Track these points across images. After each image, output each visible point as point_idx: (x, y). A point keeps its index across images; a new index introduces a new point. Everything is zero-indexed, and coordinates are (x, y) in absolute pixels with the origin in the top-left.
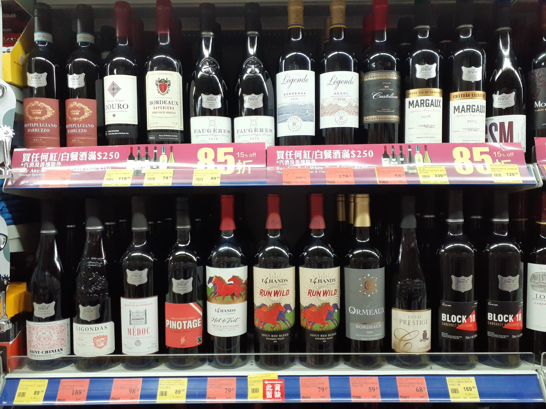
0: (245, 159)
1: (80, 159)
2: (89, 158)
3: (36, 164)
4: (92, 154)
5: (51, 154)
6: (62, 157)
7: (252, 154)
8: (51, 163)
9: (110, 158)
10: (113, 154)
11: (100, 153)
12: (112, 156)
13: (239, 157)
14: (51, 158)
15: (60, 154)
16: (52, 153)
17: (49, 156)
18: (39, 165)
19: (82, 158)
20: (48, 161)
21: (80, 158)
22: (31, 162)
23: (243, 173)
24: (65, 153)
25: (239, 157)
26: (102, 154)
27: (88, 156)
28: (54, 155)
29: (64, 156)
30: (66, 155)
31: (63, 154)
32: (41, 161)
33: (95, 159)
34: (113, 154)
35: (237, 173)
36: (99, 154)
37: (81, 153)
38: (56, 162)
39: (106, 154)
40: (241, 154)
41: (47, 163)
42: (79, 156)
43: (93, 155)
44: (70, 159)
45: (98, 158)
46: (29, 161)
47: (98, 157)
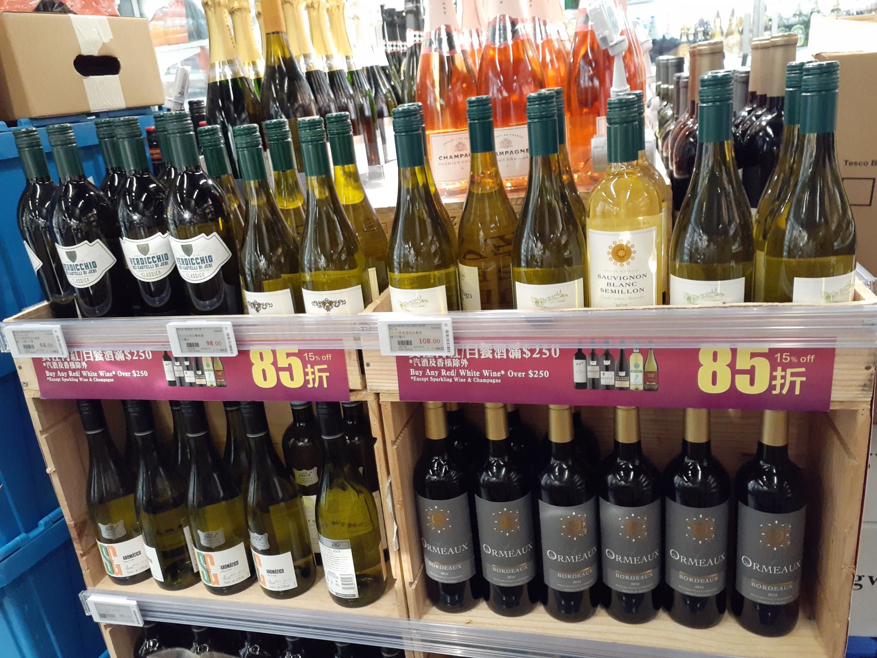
0: (791, 365)
1: (496, 357)
2: (510, 354)
3: (431, 362)
7: (806, 357)
9: (544, 356)
13: (779, 361)
18: (436, 364)
19: (499, 354)
23: (784, 392)
25: (779, 361)
35: (774, 392)
38: (460, 359)
40: (784, 357)
45: (524, 355)
47: (525, 353)
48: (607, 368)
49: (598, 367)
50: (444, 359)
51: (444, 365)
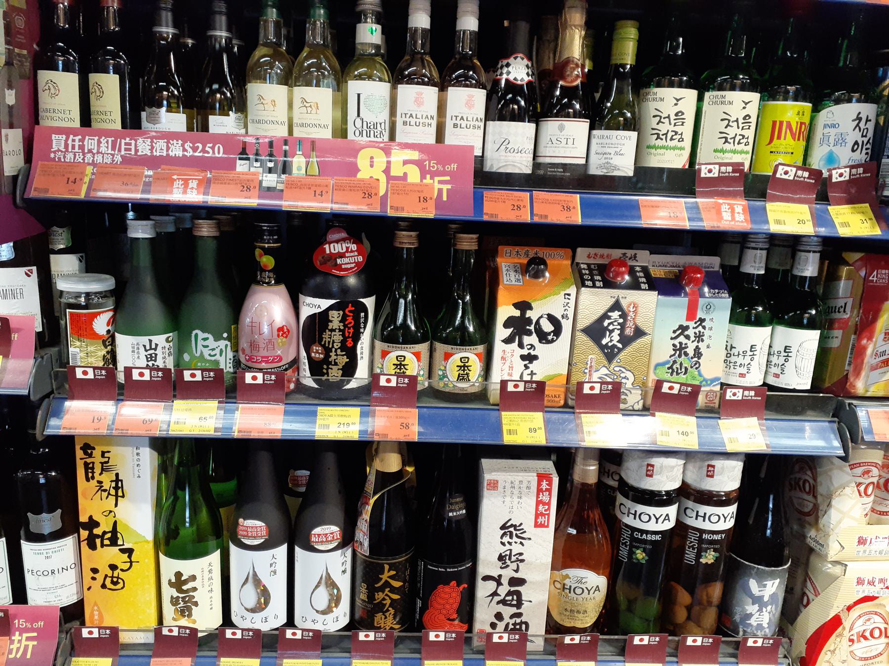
3: (77, 157)
4: (175, 145)
5: (102, 140)
6: (123, 147)
8: (103, 157)
9: (206, 155)
10: (213, 148)
11: (189, 143)
12: (210, 151)
14: (103, 149)
16: (103, 138)
17: (99, 142)
18: (83, 159)
19: (158, 151)
20: (98, 152)
21: (154, 151)
24: (128, 140)
26: (194, 144)
27: (168, 148)
28: (107, 142)
29: (126, 144)
30: (130, 144)
31: (123, 141)
32: (86, 151)
33: (181, 155)
34: (213, 148)
36: (188, 146)
37: (155, 141)
38: (113, 155)
39: (200, 146)
41: (96, 156)
42: (152, 148)
43: (177, 148)
44: (137, 151)
46: (64, 150)
47: (186, 151)
48: (270, 171)
49: (261, 169)
50: (94, 154)
51: (93, 161)
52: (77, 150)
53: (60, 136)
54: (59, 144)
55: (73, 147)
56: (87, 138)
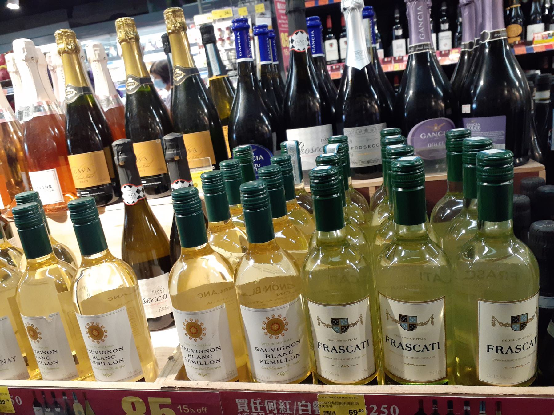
5: (280, 403)
6: (300, 408)
15: (295, 402)
17: (277, 403)
22: (252, 412)
24: (303, 402)
31: (299, 404)
52: (259, 411)
53: (243, 400)
54: (242, 406)
55: (256, 408)
56: (266, 401)
